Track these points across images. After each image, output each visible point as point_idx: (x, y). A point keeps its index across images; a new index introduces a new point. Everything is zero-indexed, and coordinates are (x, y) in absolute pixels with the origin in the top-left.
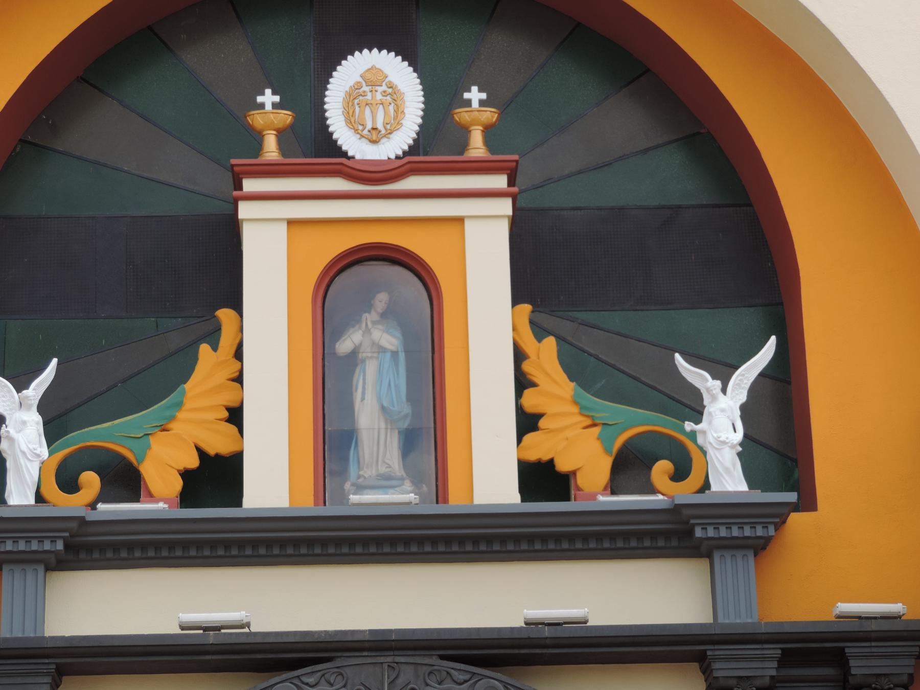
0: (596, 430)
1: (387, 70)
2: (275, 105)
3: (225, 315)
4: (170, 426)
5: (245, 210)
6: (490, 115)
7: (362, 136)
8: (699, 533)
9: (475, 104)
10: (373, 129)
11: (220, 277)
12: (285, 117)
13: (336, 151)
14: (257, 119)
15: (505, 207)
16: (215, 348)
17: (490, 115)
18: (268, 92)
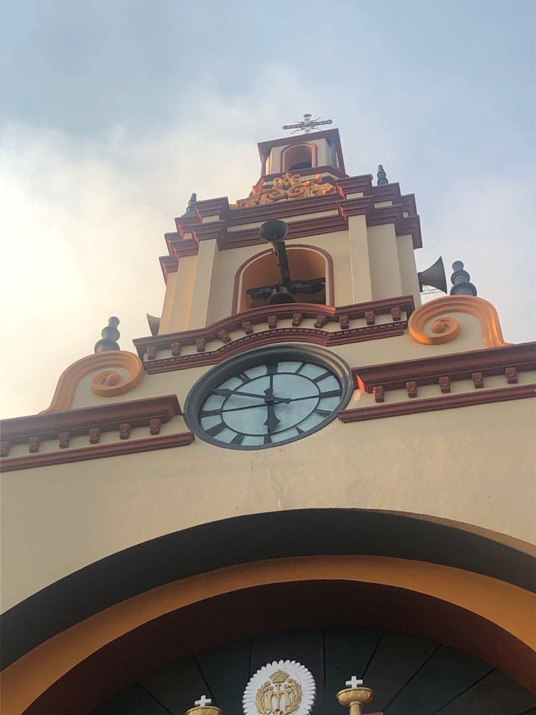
2: (206, 704)
6: (365, 694)
9: (354, 686)
10: (277, 710)
17: (365, 694)
18: (203, 697)
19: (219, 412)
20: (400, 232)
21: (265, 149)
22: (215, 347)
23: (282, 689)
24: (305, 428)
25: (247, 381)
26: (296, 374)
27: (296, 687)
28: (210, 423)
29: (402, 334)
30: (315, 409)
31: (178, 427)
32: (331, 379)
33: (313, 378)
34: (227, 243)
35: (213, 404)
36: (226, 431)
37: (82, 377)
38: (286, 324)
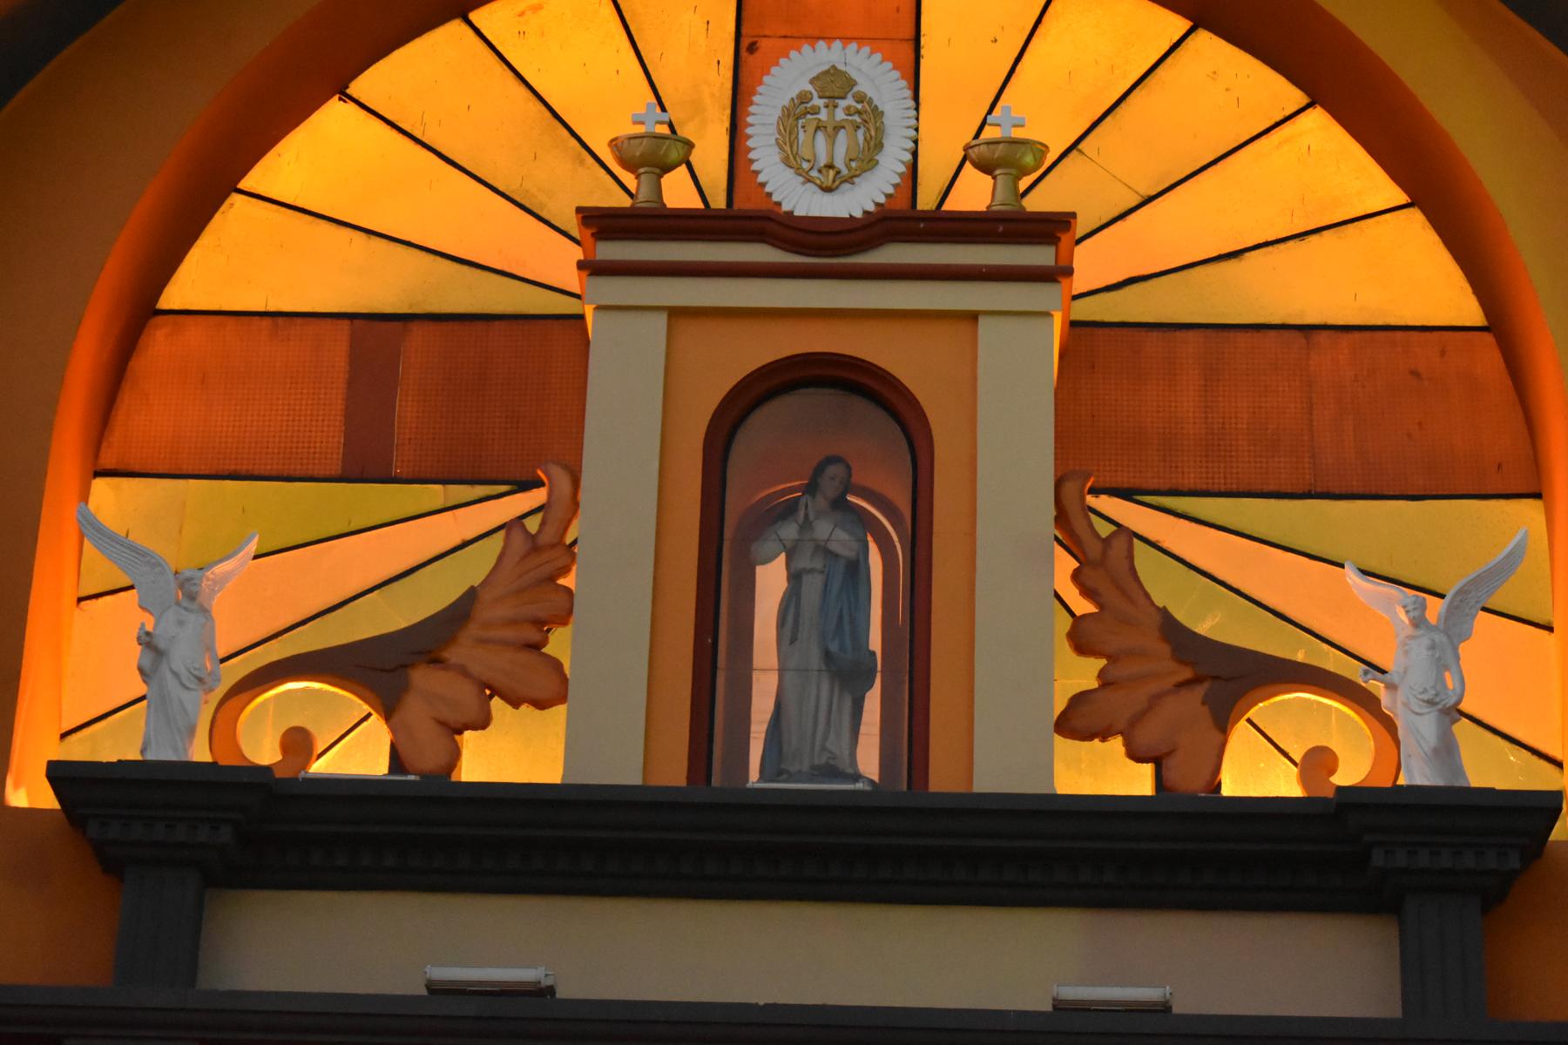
0: (1200, 690)
1: (854, 75)
4: (445, 655)
7: (809, 180)
8: (1378, 859)
10: (830, 166)
23: (840, 115)
27: (870, 116)
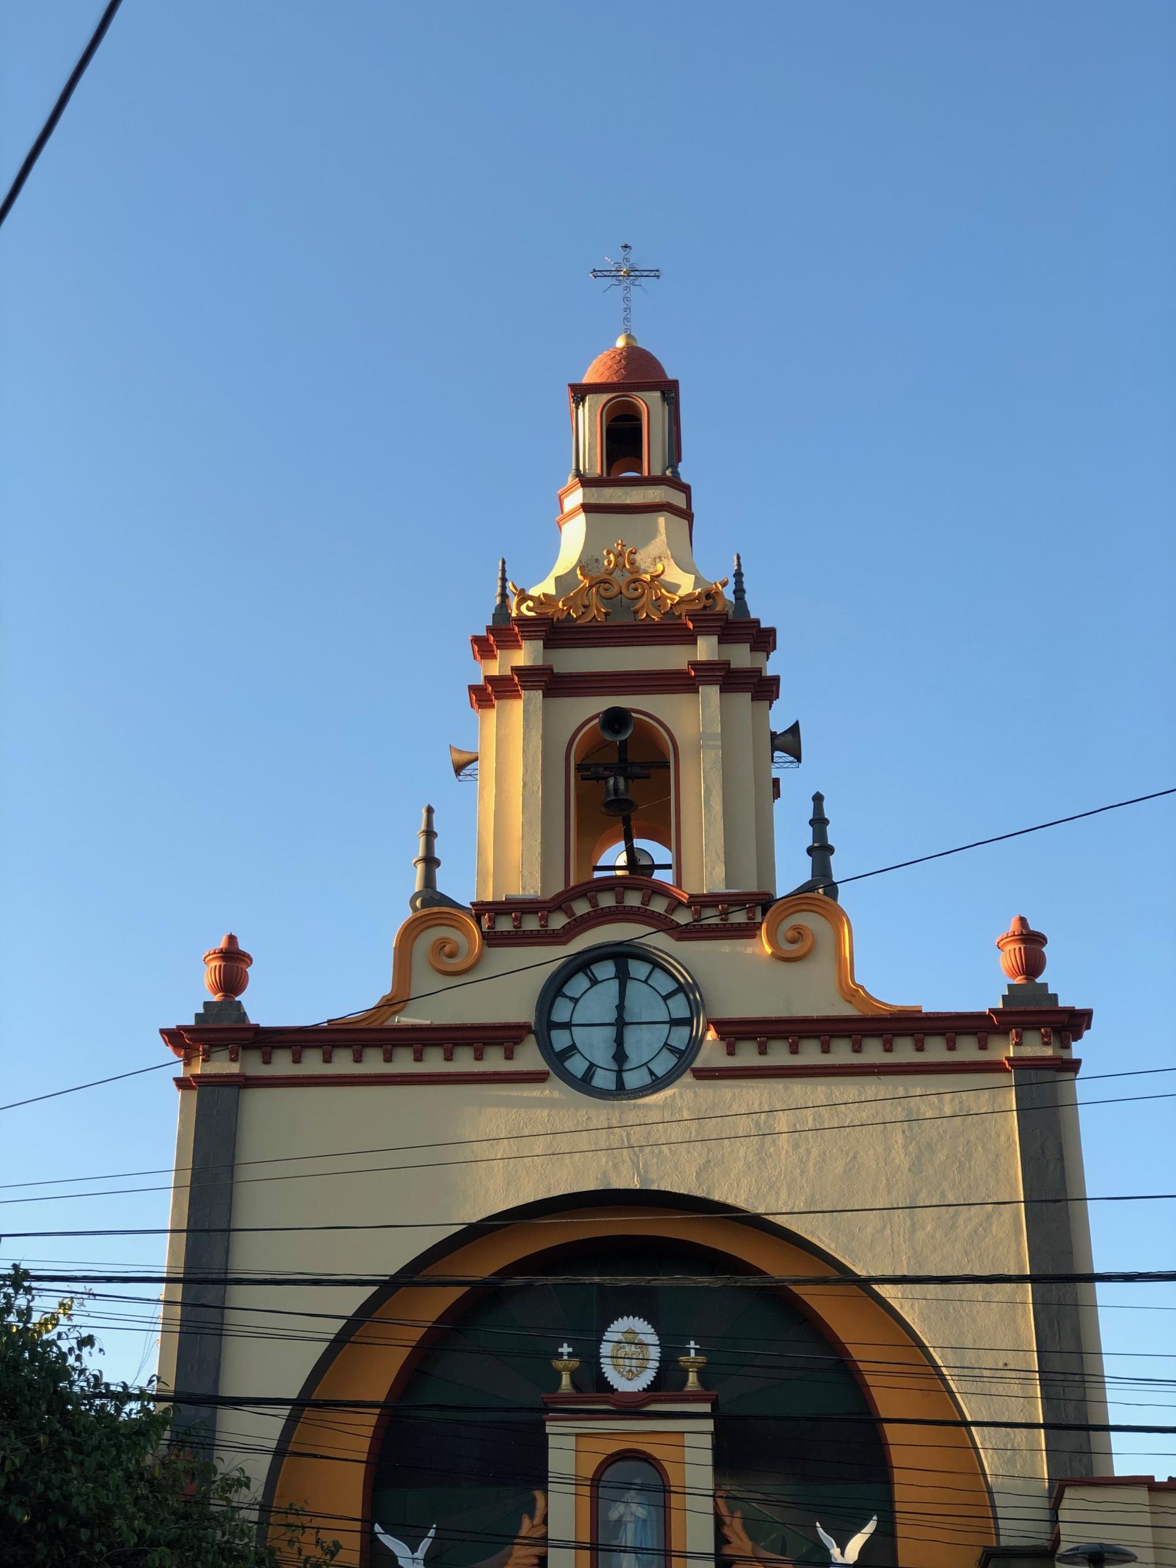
3: (538, 1495)
5: (548, 1430)
11: (534, 1473)
12: (575, 1363)
13: (609, 1388)
14: (558, 1364)
15: (709, 1425)
16: (532, 1517)
18: (565, 1345)
19: (567, 1026)
20: (754, 699)
21: (580, 392)
22: (558, 921)
24: (660, 1071)
25: (594, 982)
26: (646, 982)
28: (560, 1039)
29: (753, 936)
30: (666, 1043)
31: (530, 1057)
32: (681, 997)
33: (664, 994)
34: (552, 684)
35: (561, 1013)
36: (577, 1057)
37: (415, 938)
38: (633, 900)
